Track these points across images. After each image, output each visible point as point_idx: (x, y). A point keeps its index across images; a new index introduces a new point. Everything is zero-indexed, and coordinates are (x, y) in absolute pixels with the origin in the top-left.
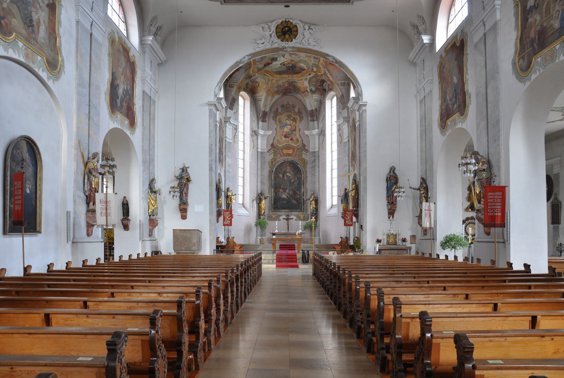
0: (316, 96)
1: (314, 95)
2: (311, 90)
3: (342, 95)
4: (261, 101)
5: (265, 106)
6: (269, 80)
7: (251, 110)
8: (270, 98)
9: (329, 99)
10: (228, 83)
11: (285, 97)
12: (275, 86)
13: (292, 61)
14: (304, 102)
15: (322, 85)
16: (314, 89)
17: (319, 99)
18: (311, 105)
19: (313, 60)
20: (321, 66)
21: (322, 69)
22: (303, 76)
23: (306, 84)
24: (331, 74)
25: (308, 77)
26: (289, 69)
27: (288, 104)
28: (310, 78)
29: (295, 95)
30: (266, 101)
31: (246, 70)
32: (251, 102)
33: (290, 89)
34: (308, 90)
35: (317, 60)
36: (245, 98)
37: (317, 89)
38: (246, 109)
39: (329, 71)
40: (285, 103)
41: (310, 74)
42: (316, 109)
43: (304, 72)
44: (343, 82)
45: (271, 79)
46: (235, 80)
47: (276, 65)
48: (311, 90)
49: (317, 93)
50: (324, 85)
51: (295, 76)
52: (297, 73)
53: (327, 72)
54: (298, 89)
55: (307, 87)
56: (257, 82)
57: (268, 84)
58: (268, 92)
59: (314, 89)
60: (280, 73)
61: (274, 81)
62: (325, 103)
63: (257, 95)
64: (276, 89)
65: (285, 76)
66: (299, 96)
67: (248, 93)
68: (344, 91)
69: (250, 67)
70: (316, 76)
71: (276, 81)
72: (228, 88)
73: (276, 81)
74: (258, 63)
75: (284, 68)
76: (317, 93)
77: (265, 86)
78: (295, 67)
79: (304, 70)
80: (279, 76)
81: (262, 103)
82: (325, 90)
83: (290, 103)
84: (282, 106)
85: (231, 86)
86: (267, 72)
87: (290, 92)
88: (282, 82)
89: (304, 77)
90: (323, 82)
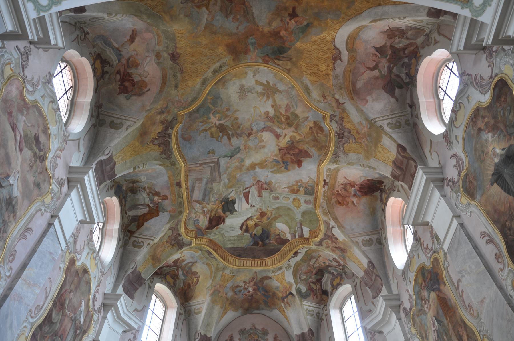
0: (309, 305)
1: (305, 302)
2: (299, 291)
3: (370, 262)
4: (200, 313)
5: (207, 325)
6: (217, 269)
7: (176, 326)
8: (217, 310)
9: (335, 308)
10: (133, 239)
11: (248, 316)
12: (229, 284)
13: (263, 214)
14: (285, 324)
15: (319, 281)
16: (304, 289)
17: (316, 310)
18: (299, 324)
19: (303, 198)
20: (319, 212)
21: (322, 217)
22: (282, 258)
23: (289, 277)
24: (341, 227)
25: (294, 261)
26: (256, 244)
27: (253, 328)
28: (297, 265)
29: (267, 313)
30: (209, 313)
31: (172, 218)
32: (179, 314)
33: (257, 301)
34: (294, 292)
35: (311, 198)
36: (168, 303)
37: (310, 289)
38: (166, 325)
39: (335, 219)
40: (248, 327)
41: (296, 254)
42: (310, 330)
43: (285, 248)
44: (367, 238)
45: (221, 266)
46: (147, 233)
47: (233, 223)
48: (299, 291)
49: (311, 298)
50: (323, 281)
51: (268, 260)
52: (270, 253)
53: (332, 223)
54: (274, 294)
55: (291, 286)
56: (195, 273)
57: (215, 277)
58: (215, 293)
59: (304, 289)
60: (240, 253)
61: (227, 272)
62: (328, 316)
63: (193, 302)
64: (230, 294)
65: (249, 262)
66: (276, 313)
67: (175, 295)
68: (372, 256)
69: (181, 213)
70: (308, 257)
71: (232, 272)
72: (130, 247)
73: (232, 272)
74: (198, 207)
75: (246, 241)
76: (311, 298)
77: (209, 283)
78: (268, 237)
79: (284, 242)
80: (237, 261)
81: (200, 319)
82: (325, 293)
83: (257, 327)
84: (242, 332)
85: (137, 245)
86: (213, 244)
87: (258, 309)
88: (243, 278)
89: (285, 262)
90: (321, 272)
